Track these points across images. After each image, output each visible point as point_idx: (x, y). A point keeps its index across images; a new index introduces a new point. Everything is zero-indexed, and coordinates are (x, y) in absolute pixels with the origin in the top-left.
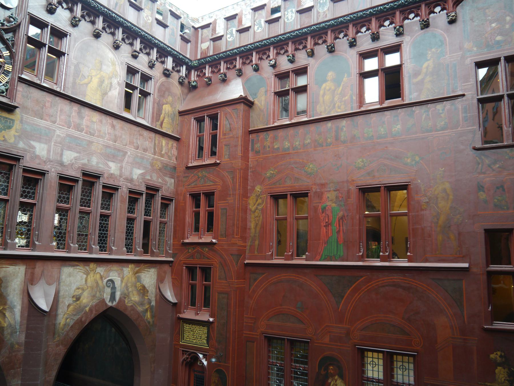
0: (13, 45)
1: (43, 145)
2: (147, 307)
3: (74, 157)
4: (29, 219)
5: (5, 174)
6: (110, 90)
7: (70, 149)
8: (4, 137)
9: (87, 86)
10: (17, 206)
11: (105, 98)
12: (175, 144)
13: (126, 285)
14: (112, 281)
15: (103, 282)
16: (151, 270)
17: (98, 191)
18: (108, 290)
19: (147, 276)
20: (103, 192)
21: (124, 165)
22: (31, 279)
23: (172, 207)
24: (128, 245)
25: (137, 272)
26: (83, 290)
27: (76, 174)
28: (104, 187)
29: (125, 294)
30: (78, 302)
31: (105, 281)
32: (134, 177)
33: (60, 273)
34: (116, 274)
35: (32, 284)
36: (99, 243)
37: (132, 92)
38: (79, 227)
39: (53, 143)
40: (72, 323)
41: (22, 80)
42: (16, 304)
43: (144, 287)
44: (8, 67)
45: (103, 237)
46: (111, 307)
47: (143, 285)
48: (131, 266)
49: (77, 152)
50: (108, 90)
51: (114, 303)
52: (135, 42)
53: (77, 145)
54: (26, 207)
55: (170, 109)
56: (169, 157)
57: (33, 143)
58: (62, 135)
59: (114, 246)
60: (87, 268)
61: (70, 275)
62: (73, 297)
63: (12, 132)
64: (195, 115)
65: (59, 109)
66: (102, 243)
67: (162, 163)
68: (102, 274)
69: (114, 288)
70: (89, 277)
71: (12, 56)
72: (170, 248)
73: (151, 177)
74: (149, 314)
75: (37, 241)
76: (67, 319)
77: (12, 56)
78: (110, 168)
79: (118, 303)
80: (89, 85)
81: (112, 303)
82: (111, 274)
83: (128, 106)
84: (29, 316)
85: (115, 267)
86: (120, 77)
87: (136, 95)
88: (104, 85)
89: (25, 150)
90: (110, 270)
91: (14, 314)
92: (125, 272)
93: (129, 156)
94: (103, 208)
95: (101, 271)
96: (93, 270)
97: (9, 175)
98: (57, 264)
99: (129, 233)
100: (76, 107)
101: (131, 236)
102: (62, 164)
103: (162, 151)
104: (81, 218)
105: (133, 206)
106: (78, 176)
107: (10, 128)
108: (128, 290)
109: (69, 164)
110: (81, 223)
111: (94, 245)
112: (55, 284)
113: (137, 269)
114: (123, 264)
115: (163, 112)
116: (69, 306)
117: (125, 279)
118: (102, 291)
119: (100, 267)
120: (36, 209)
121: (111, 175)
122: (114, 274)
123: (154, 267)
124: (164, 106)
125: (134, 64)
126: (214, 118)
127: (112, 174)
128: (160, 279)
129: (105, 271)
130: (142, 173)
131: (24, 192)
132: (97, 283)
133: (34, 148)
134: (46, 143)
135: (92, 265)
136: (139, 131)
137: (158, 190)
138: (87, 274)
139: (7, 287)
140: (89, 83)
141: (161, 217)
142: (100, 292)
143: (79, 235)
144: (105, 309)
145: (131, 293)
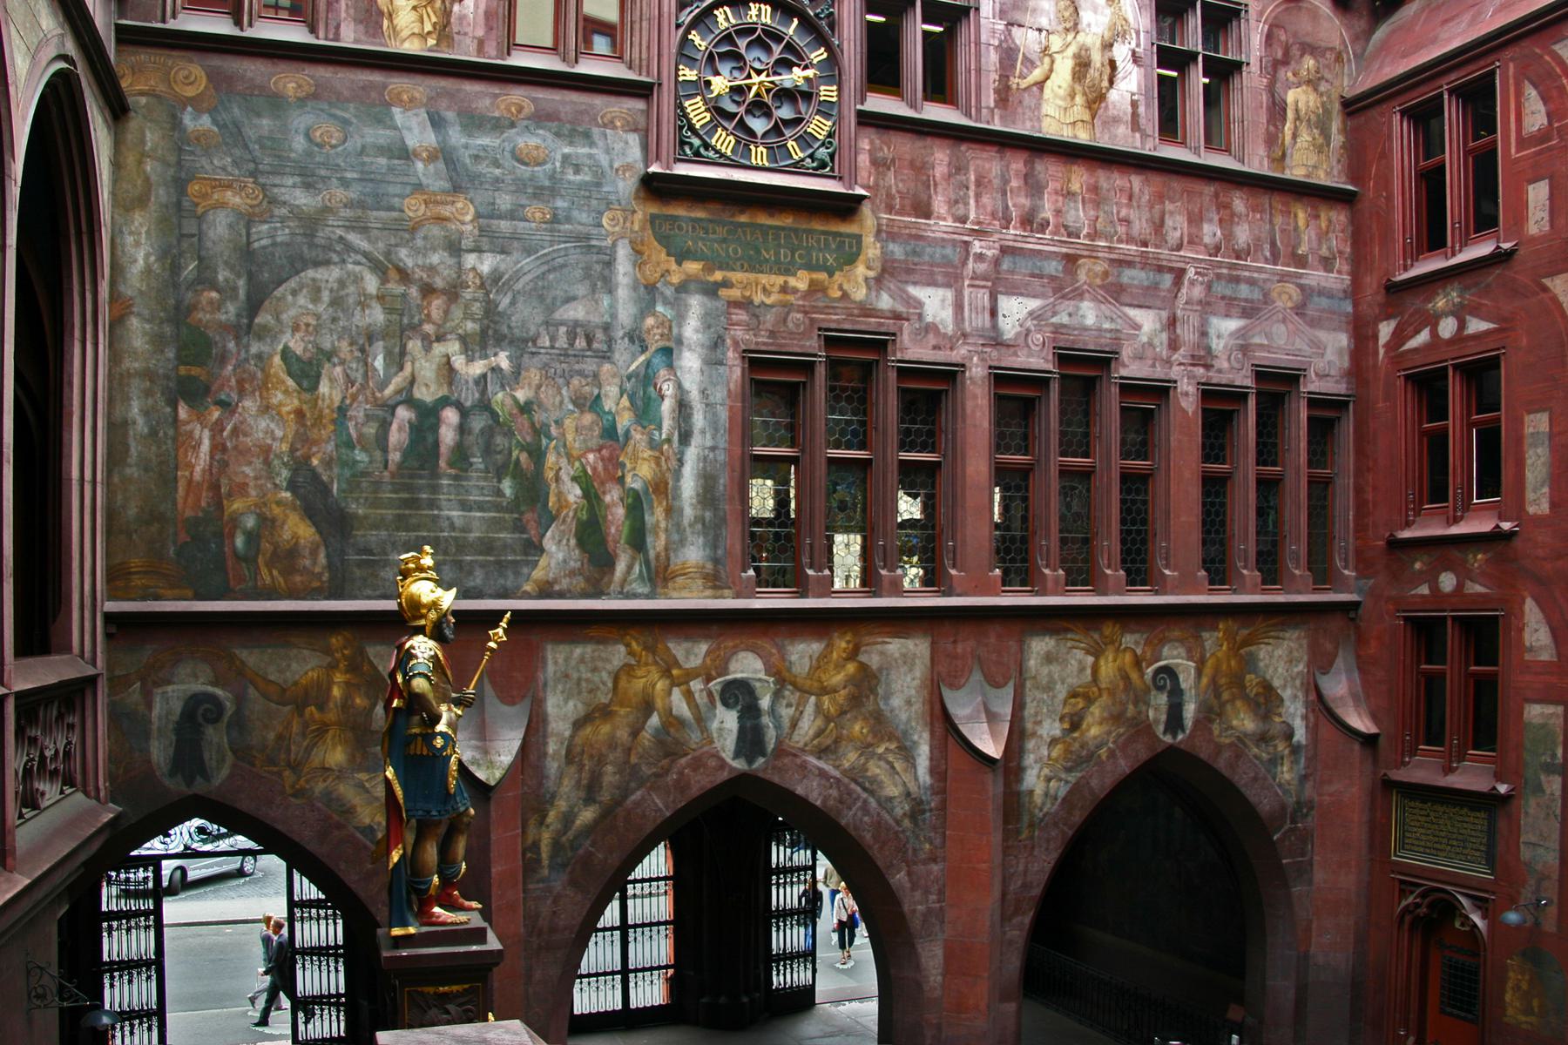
0: (832, 26)
1: (941, 292)
3: (1031, 314)
4: (926, 508)
5: (855, 390)
6: (1111, 82)
7: (1014, 290)
8: (840, 288)
9: (1041, 89)
10: (893, 475)
11: (1100, 112)
12: (1338, 217)
13: (1214, 681)
14: (1169, 671)
15: (1142, 675)
16: (1287, 635)
17: (1111, 404)
18: (1162, 699)
20: (1122, 408)
21: (1179, 312)
23: (1347, 429)
24: (1213, 561)
25: (1247, 642)
26: (1090, 701)
27: (1036, 359)
30: (1076, 735)
31: (1150, 671)
32: (1214, 346)
33: (1021, 651)
34: (1182, 651)
36: (1124, 561)
38: (1062, 518)
39: (967, 283)
41: (868, 120)
44: (827, 92)
45: (1134, 542)
47: (1265, 680)
50: (1105, 84)
53: (1033, 275)
54: (916, 478)
57: (916, 291)
58: (989, 253)
59: (1167, 567)
64: (1401, 99)
65: (973, 178)
66: (1133, 561)
68: (1139, 651)
69: (1176, 694)
70: (1102, 662)
71: (833, 60)
72: (1346, 560)
75: (954, 566)
76: (1049, 780)
77: (833, 60)
78: (1138, 327)
79: (1192, 736)
80: (1049, 83)
83: (1169, 125)
86: (1138, 33)
87: (1198, 79)
88: (1092, 73)
89: (897, 317)
90: (1163, 641)
91: (914, 767)
92: (1208, 644)
93: (1192, 283)
94: (1125, 455)
95: (1137, 643)
96: (1112, 642)
97: (865, 390)
99: (1213, 523)
101: (1217, 532)
104: (1065, 492)
105: (1217, 437)
107: (852, 260)
109: (1018, 334)
110: (1068, 506)
111: (1109, 567)
112: (1011, 684)
113: (1245, 632)
117: (1210, 663)
118: (1141, 698)
120: (943, 478)
123: (1296, 626)
126: (1479, 100)
128: (1321, 662)
129: (1148, 642)
130: (1239, 330)
131: (907, 432)
132: (1126, 678)
133: (919, 304)
134: (947, 285)
135: (1108, 629)
136: (1216, 195)
138: (1097, 653)
140: (1048, 78)
141: (1310, 464)
142: (1136, 704)
143: (1063, 541)
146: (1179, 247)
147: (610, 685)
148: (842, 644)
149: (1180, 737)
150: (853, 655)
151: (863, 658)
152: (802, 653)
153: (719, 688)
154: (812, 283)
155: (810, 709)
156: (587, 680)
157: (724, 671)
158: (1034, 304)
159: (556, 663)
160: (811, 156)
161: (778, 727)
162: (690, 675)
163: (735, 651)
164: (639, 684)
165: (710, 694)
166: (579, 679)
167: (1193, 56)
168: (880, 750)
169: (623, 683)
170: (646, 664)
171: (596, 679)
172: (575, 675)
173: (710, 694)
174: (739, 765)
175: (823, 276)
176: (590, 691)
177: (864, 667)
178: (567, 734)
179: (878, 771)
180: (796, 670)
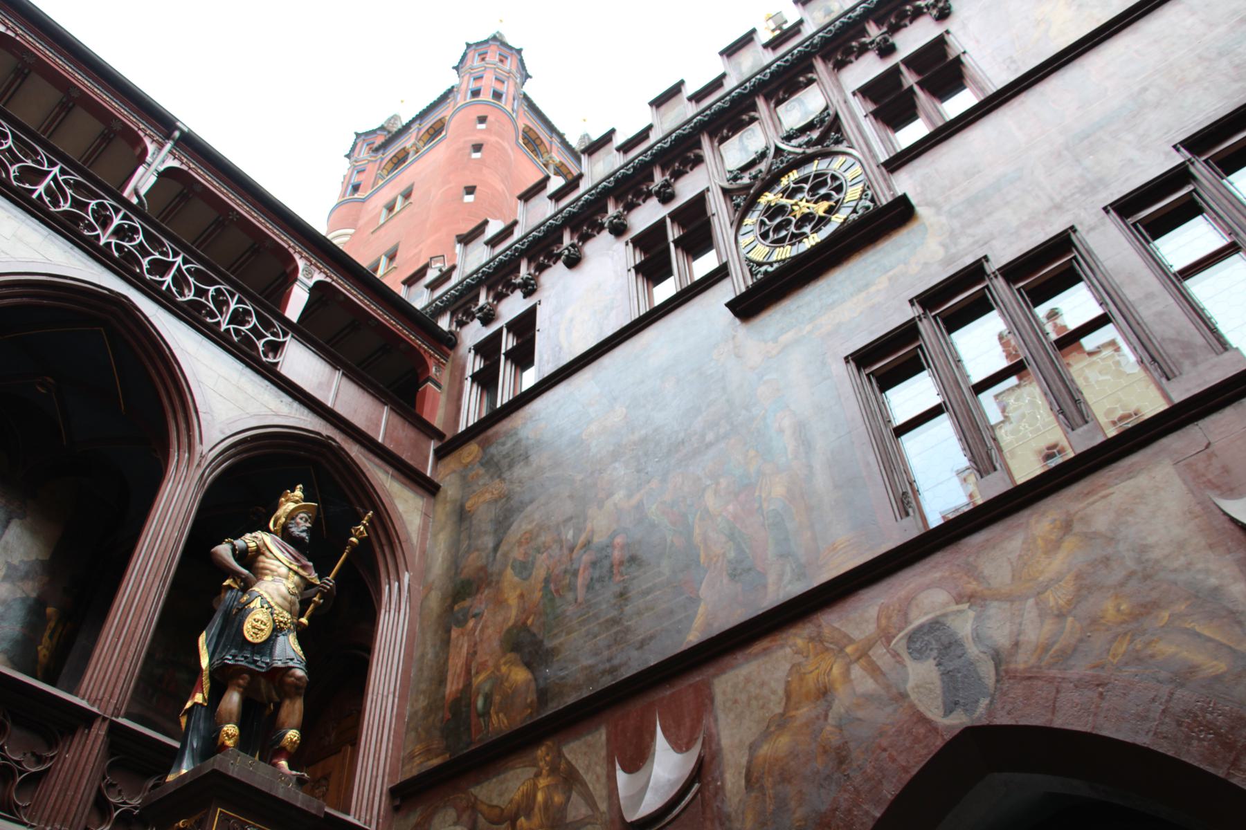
42: (1213, 581)
147: (781, 692)
153: (904, 641)
154: (890, 279)
156: (756, 698)
157: (906, 620)
159: (724, 693)
160: (854, 211)
162: (870, 644)
164: (811, 679)
165: (896, 655)
166: (749, 700)
169: (795, 685)
170: (816, 655)
171: (766, 691)
172: (743, 697)
173: (896, 655)
174: (958, 720)
176: (762, 707)
178: (744, 761)
179: (1171, 649)
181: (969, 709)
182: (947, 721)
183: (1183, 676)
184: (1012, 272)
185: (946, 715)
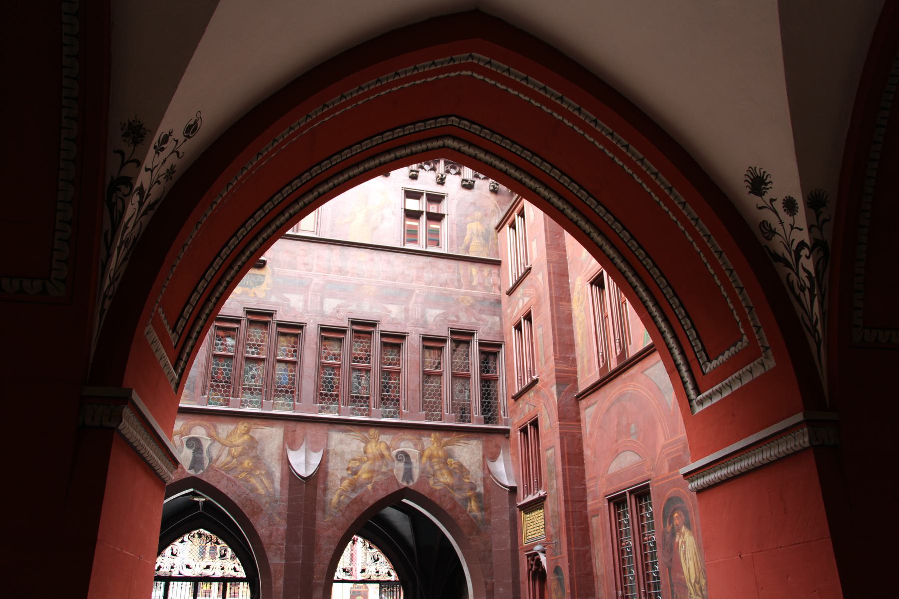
2: (469, 494)
7: (332, 296)
14: (402, 452)
16: (471, 442)
19: (465, 450)
21: (410, 306)
22: (291, 443)
25: (446, 444)
28: (383, 335)
29: (428, 473)
31: (394, 453)
34: (411, 444)
35: (292, 449)
37: (438, 227)
40: (347, 501)
43: (461, 466)
46: (406, 489)
48: (434, 435)
49: (341, 299)
51: (411, 484)
52: (437, 166)
55: (480, 227)
56: (485, 288)
57: (286, 295)
60: (366, 435)
61: (341, 442)
62: (348, 469)
63: (263, 287)
67: (473, 297)
68: (388, 443)
70: (369, 446)
73: (457, 316)
74: (473, 505)
78: (390, 312)
81: (408, 483)
82: (402, 444)
84: (290, 485)
85: (408, 435)
89: (276, 304)
90: (402, 440)
93: (417, 295)
96: (374, 438)
98: (326, 427)
100: (338, 249)
102: (323, 315)
103: (471, 282)
106: (346, 325)
107: (260, 283)
108: (432, 467)
113: (446, 439)
114: (422, 432)
115: (468, 233)
116: (343, 479)
119: (384, 433)
121: (393, 322)
122: (407, 444)
123: (476, 439)
124: (468, 226)
125: (415, 186)
127: (393, 319)
133: (288, 300)
135: (373, 431)
137: (472, 334)
139: (263, 450)
144: (397, 489)
145: (438, 473)
146: (412, 281)
148: (242, 426)
149: (411, 484)
150: (247, 432)
151: (251, 434)
152: (225, 429)
155: (226, 452)
158: (339, 302)
161: (211, 459)
163: (194, 426)
165: (182, 442)
167: (422, 212)
168: (258, 472)
173: (182, 442)
174: (192, 473)
175: (248, 289)
177: (252, 438)
180: (220, 436)
181: (196, 471)
182: (189, 472)
183: (254, 489)
184: (280, 325)
185: (190, 469)
